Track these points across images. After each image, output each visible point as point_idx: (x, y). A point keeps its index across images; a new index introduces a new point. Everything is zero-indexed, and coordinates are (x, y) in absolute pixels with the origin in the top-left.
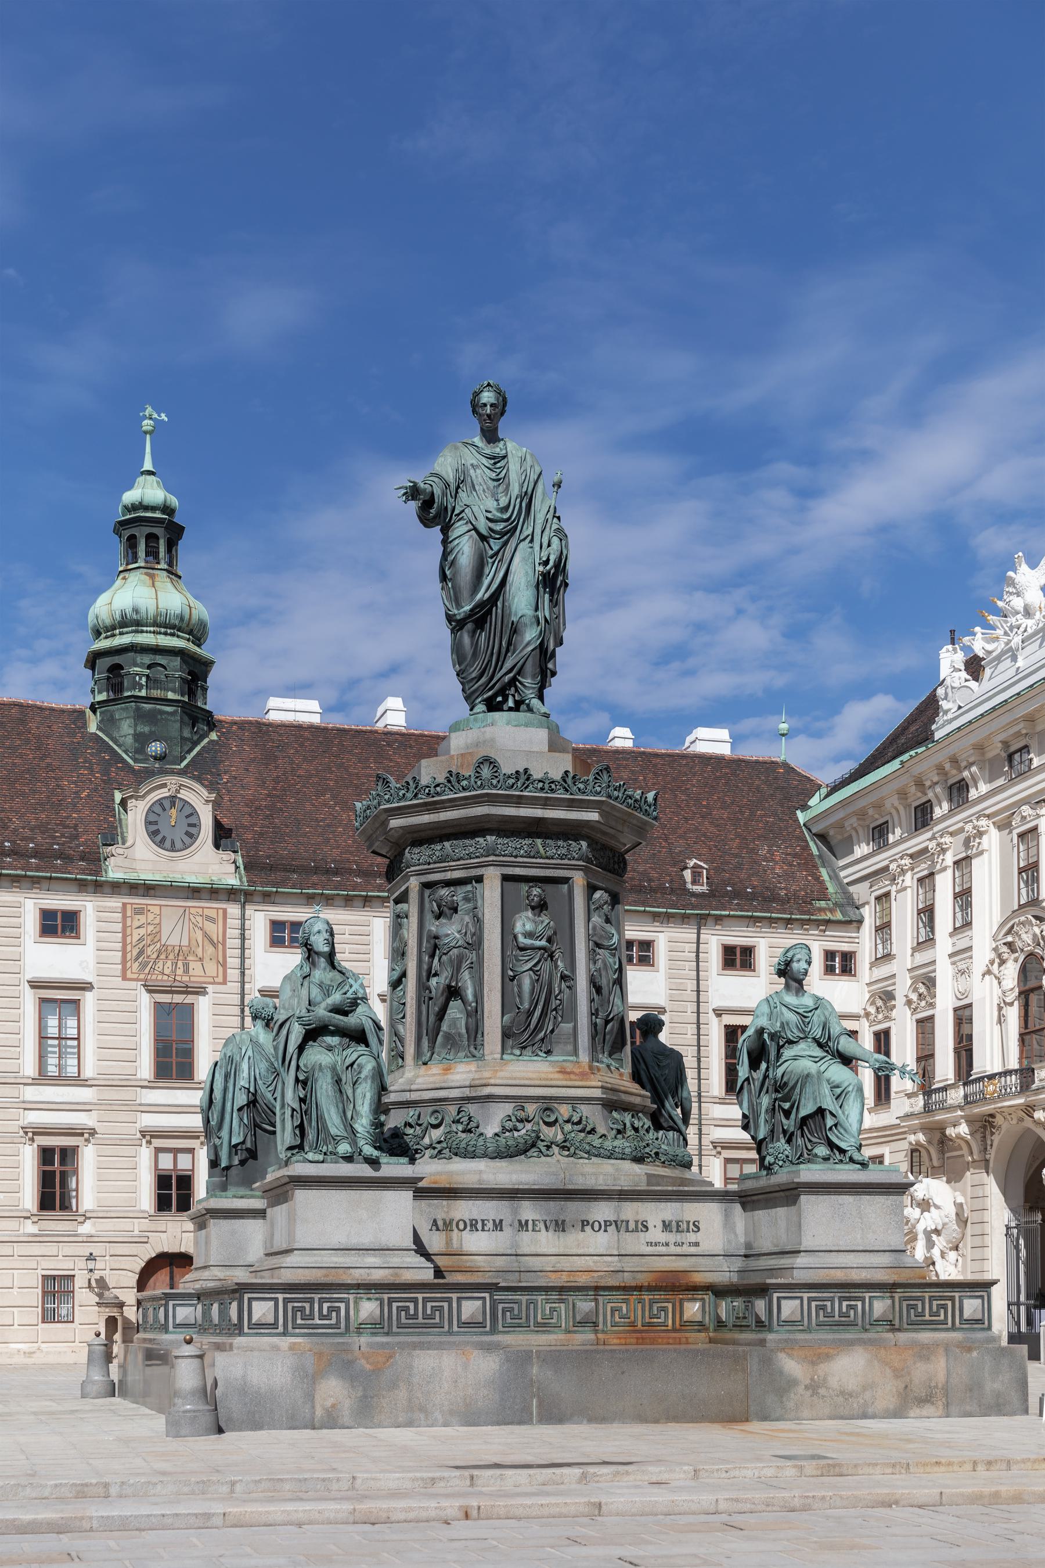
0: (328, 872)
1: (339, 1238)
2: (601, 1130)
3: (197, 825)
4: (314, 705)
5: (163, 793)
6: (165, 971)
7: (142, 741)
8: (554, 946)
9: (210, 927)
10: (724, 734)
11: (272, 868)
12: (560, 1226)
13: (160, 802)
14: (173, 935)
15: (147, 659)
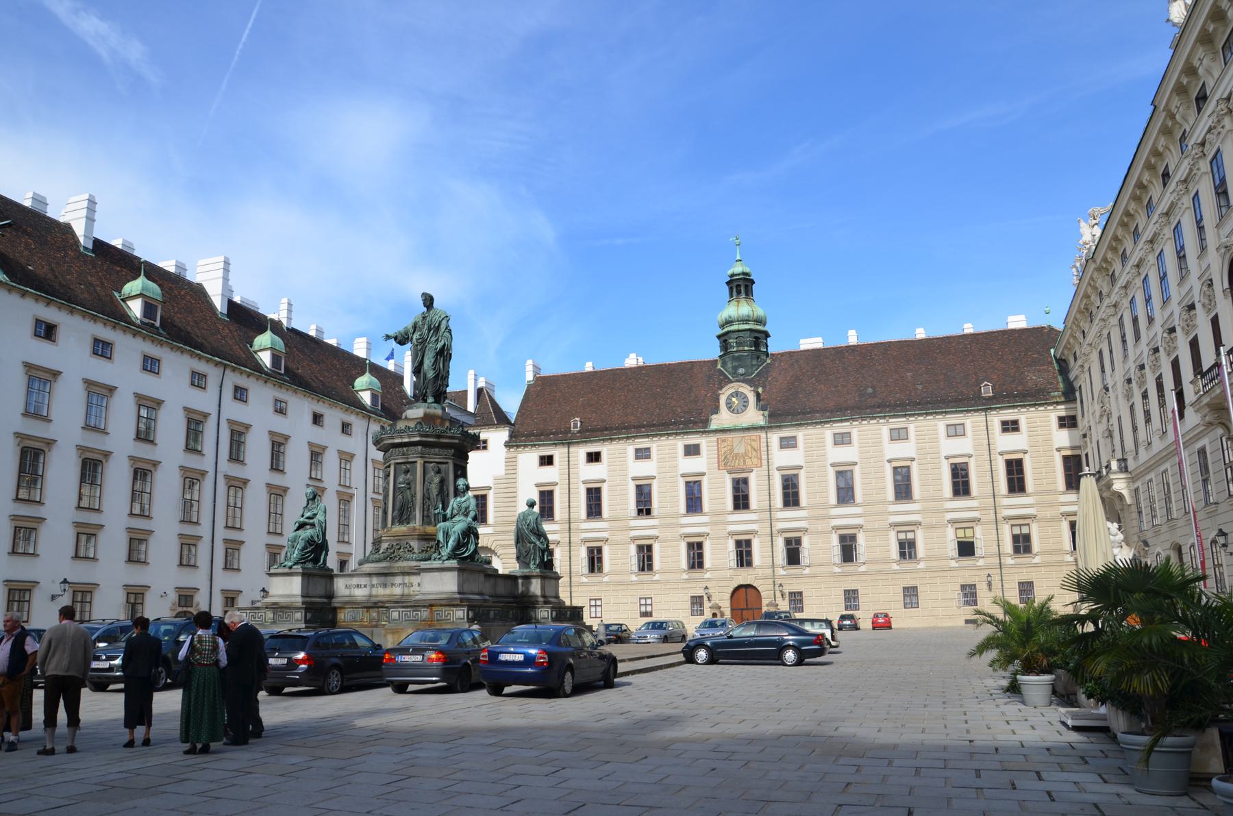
0: (804, 414)
1: (281, 592)
2: (416, 550)
3: (747, 402)
4: (820, 339)
5: (733, 390)
6: (738, 464)
7: (735, 368)
8: (410, 485)
9: (755, 444)
10: (1022, 317)
11: (780, 415)
12: (385, 586)
13: (732, 395)
14: (739, 449)
15: (736, 335)
